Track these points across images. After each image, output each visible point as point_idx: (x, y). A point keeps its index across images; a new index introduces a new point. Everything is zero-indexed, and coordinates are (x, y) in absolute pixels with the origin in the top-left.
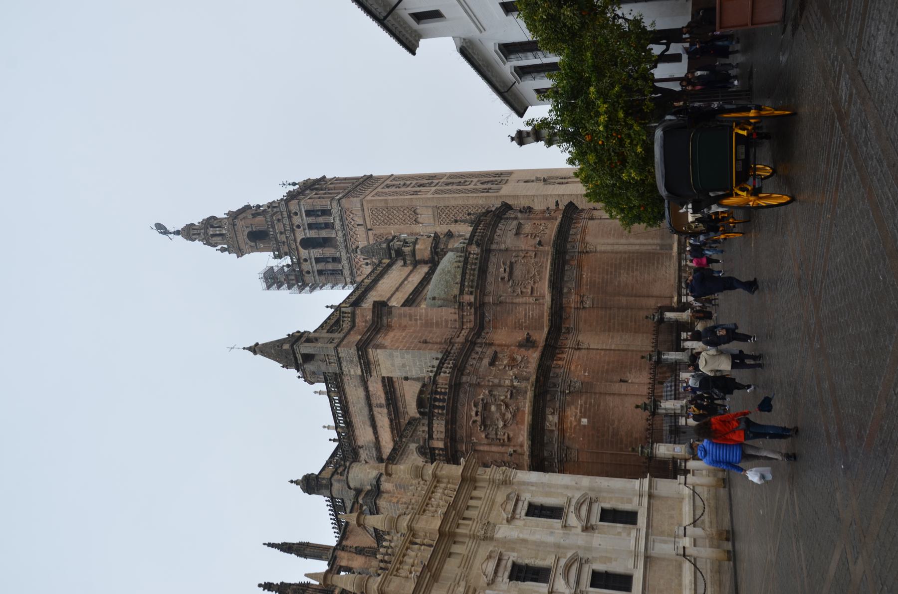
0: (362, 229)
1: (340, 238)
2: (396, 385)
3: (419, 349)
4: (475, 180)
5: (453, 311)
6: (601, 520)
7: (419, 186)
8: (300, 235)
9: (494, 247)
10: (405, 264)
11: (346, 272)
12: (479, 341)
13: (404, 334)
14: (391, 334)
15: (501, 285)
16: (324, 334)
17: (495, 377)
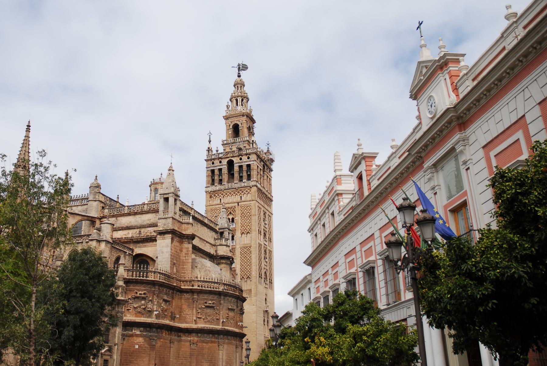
0: (239, 200)
1: (234, 185)
2: (151, 244)
3: (171, 261)
4: (268, 268)
5: (190, 277)
6: (104, 360)
7: (265, 234)
8: (236, 160)
9: (222, 297)
10: (215, 239)
11: (213, 188)
12: (175, 292)
13: (178, 251)
14: (178, 244)
15: (203, 302)
16: (179, 205)
17: (158, 302)
